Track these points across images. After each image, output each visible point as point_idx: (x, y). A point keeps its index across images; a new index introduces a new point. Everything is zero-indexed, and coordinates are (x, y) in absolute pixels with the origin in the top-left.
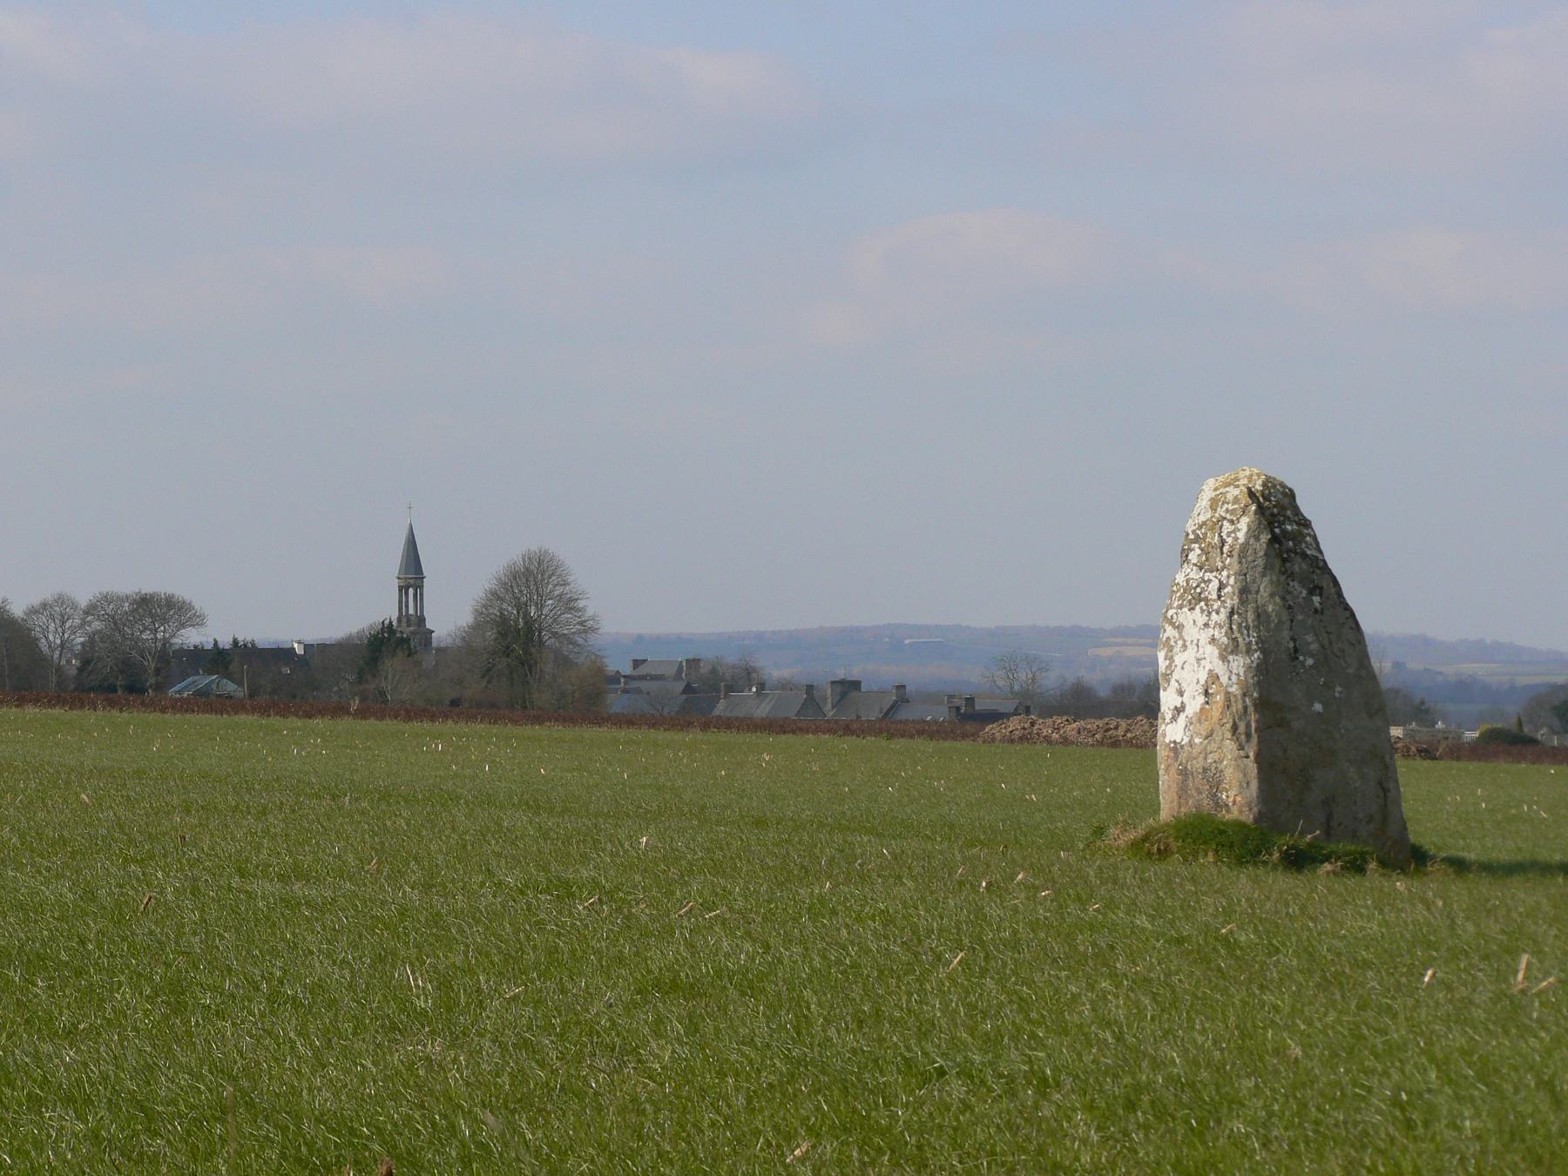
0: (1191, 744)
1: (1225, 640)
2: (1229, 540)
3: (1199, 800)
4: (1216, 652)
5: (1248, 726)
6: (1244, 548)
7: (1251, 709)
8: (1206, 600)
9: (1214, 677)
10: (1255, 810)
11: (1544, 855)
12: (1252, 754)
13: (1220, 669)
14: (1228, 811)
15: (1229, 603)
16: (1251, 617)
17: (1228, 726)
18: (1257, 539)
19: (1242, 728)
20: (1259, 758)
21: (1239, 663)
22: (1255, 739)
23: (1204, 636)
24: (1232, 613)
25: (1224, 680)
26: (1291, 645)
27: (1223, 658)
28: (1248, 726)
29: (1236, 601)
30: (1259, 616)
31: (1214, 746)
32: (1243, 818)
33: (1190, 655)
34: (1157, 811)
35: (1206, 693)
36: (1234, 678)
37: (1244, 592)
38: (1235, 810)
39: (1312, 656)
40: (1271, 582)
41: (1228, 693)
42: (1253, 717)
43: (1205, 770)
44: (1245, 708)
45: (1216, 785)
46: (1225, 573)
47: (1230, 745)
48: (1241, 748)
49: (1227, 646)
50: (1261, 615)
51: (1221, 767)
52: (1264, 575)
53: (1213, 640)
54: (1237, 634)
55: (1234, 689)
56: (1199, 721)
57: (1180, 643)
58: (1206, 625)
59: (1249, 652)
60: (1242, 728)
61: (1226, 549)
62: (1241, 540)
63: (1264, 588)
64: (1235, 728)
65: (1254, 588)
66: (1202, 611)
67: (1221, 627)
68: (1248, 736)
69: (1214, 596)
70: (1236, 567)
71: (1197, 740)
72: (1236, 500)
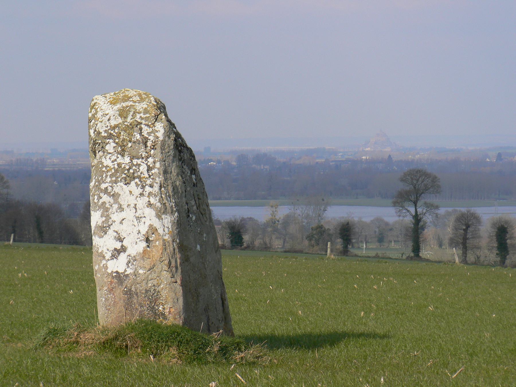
0: (135, 274)
1: (159, 205)
2: (151, 138)
3: (141, 311)
4: (153, 213)
5: (176, 262)
6: (163, 142)
7: (177, 250)
8: (139, 177)
9: (153, 230)
10: (182, 317)
11: (296, 353)
12: (179, 282)
13: (157, 223)
14: (165, 318)
15: (158, 180)
16: (170, 188)
17: (166, 262)
18: (169, 138)
19: (173, 264)
20: (184, 285)
21: (168, 220)
22: (179, 268)
23: (142, 202)
24: (161, 187)
25: (160, 231)
26: (186, 207)
27: (159, 217)
28: (176, 262)
29: (162, 178)
30: (174, 189)
31: (154, 275)
32: (176, 322)
33: (129, 214)
34: (93, 317)
35: (147, 240)
36: (166, 230)
37: (165, 172)
38: (171, 318)
39: (195, 214)
40: (177, 166)
41: (164, 240)
42: (178, 256)
43: (147, 291)
44: (174, 249)
45: (153, 298)
46: (151, 160)
47: (166, 275)
48: (173, 276)
49: (161, 208)
50: (175, 188)
51: (159, 289)
52: (173, 162)
53: (150, 205)
54: (165, 201)
55: (166, 237)
56: (143, 258)
57: (116, 206)
58: (142, 194)
59: (172, 212)
60: (173, 264)
61: (149, 144)
62: (161, 138)
63: (174, 170)
64: (170, 263)
65: (169, 171)
66: (137, 185)
67: (156, 196)
68: (177, 268)
69: (146, 175)
70: (159, 156)
71: (141, 272)
72: (146, 111)
